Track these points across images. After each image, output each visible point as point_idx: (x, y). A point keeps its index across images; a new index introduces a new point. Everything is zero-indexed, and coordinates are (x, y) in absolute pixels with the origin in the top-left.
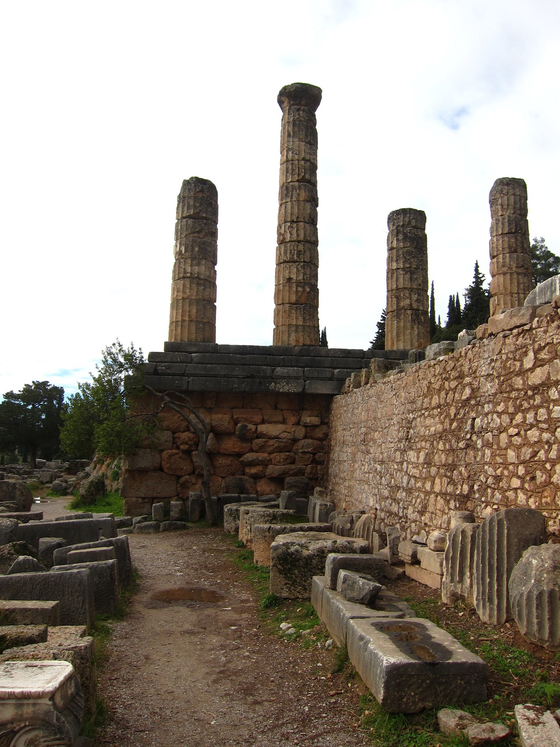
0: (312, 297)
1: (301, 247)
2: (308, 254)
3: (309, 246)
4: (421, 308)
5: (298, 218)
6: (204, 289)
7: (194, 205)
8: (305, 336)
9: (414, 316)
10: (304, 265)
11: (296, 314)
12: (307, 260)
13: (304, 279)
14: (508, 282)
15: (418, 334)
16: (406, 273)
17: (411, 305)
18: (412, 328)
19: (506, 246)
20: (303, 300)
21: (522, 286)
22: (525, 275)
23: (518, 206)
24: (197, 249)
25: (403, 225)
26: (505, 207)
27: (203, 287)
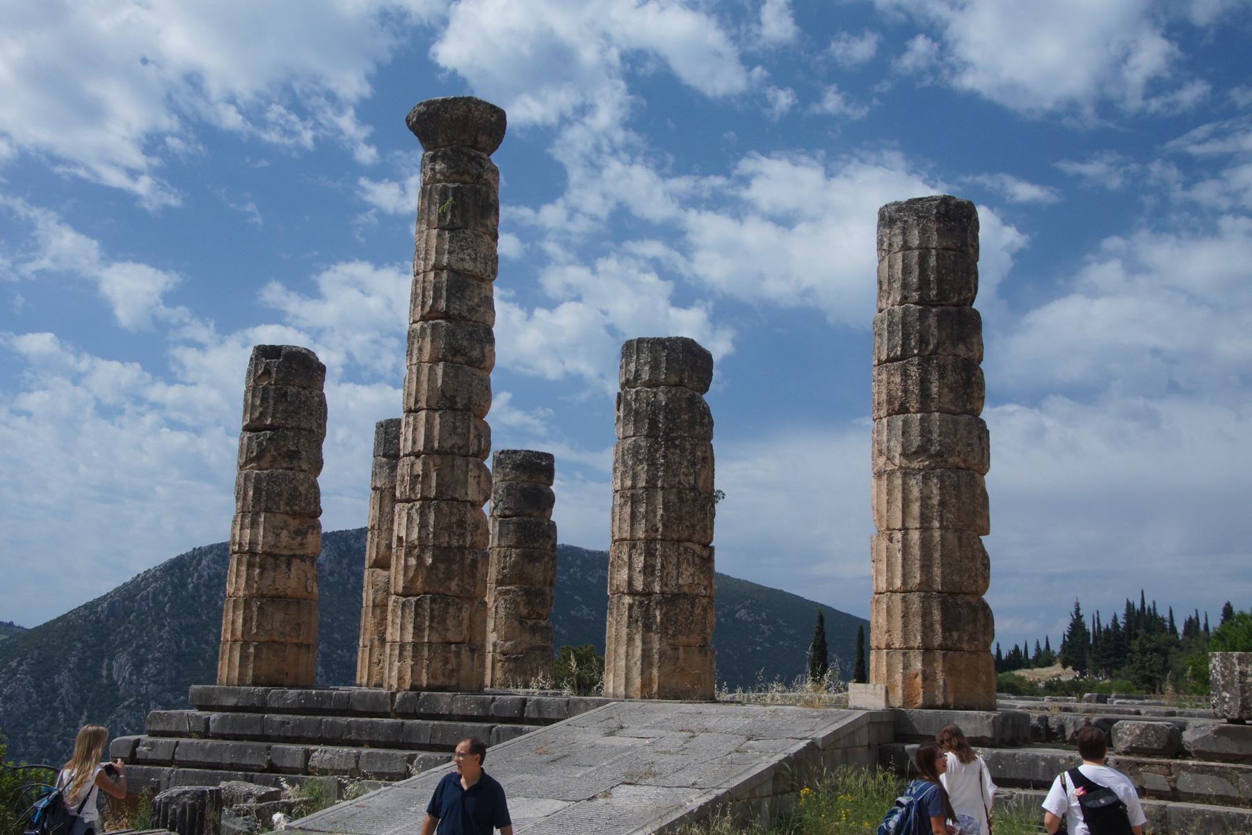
0: (441, 576)
3: (438, 460)
5: (417, 402)
6: (261, 574)
7: (253, 403)
9: (636, 611)
11: (403, 617)
13: (419, 538)
14: (885, 497)
16: (625, 503)
17: (630, 581)
18: (630, 639)
19: (884, 396)
21: (916, 508)
23: (914, 279)
24: (251, 493)
25: (627, 380)
26: (885, 287)
27: (257, 571)
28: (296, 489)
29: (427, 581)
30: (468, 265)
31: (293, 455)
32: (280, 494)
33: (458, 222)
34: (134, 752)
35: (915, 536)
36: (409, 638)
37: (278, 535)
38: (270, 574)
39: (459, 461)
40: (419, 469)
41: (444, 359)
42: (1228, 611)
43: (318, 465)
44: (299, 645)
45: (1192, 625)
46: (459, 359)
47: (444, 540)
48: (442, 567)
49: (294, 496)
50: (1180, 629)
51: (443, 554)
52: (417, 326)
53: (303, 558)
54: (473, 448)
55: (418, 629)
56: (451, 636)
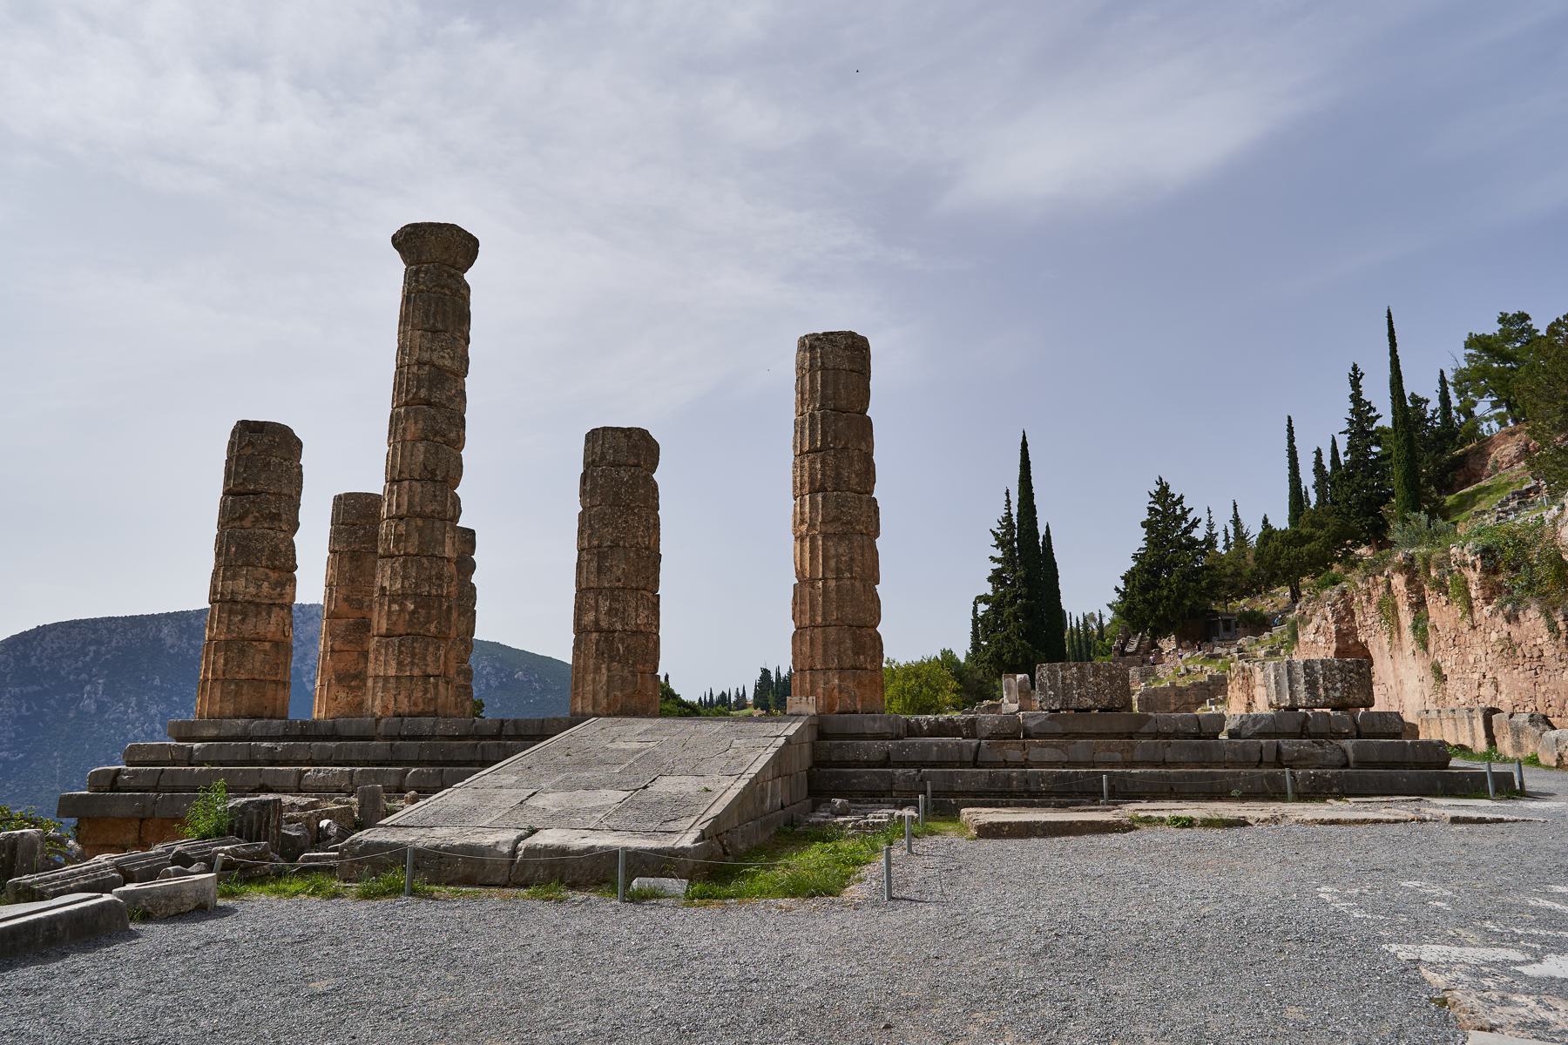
1: (402, 528)
2: (415, 539)
3: (420, 522)
4: (619, 627)
6: (243, 620)
8: (400, 698)
9: (602, 645)
10: (405, 561)
12: (410, 550)
14: (807, 555)
15: (610, 679)
17: (597, 622)
18: (597, 670)
20: (401, 629)
21: (832, 563)
22: (842, 536)
28: (277, 546)
29: (410, 623)
30: (448, 363)
31: (275, 517)
32: (262, 550)
33: (440, 326)
34: (114, 781)
35: (832, 583)
36: (392, 672)
37: (260, 586)
38: (251, 621)
39: (438, 524)
40: (402, 528)
41: (426, 438)
43: (295, 526)
44: (276, 682)
46: (438, 439)
47: (425, 589)
48: (422, 612)
49: (275, 552)
51: (424, 602)
53: (282, 607)
54: (450, 514)
55: (400, 664)
56: (430, 670)
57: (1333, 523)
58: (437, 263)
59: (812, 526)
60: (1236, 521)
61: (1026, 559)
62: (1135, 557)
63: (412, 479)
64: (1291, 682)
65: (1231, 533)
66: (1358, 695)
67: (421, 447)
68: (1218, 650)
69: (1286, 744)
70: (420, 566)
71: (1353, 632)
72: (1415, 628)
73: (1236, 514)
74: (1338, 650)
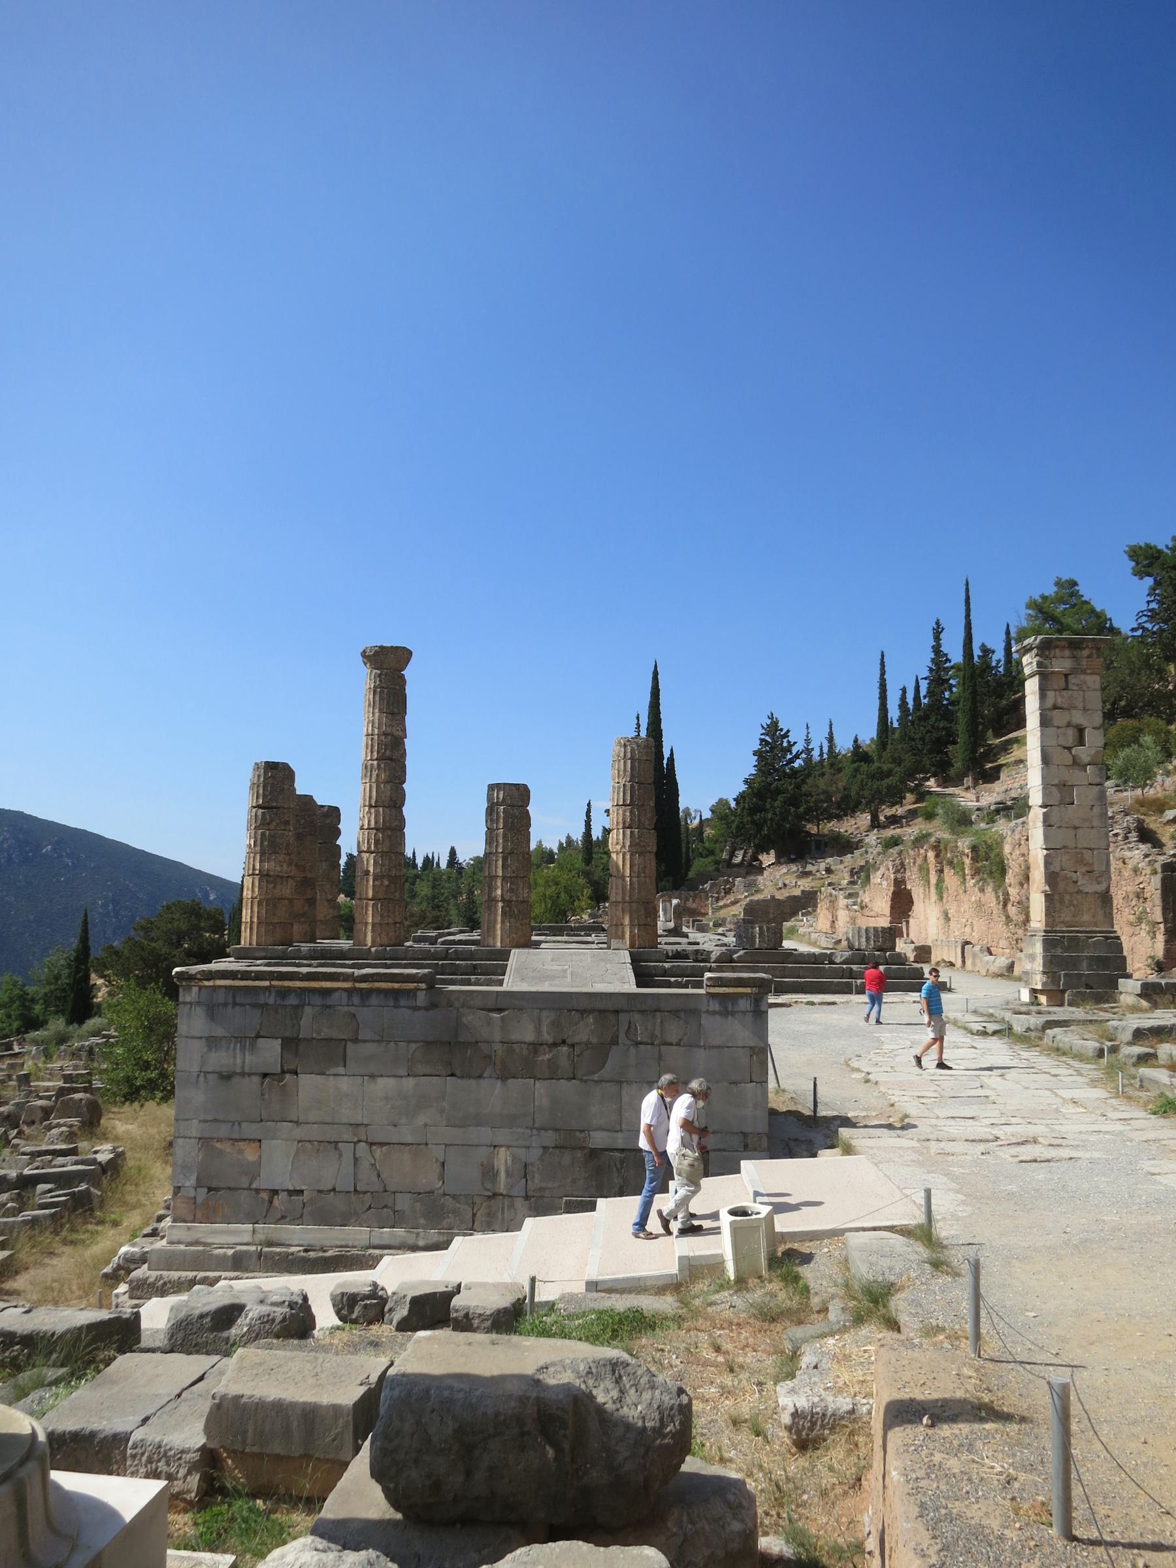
3: (389, 832)
19: (620, 819)
30: (400, 733)
33: (396, 710)
35: (635, 879)
42: (453, 853)
45: (428, 861)
47: (393, 872)
50: (420, 862)
52: (375, 763)
55: (382, 916)
57: (908, 759)
58: (389, 668)
59: (624, 846)
60: (831, 739)
61: (651, 776)
62: (746, 781)
63: (384, 807)
64: (860, 937)
65: (825, 750)
66: (888, 945)
67: (388, 786)
68: (809, 868)
69: (854, 967)
70: (390, 859)
71: (903, 882)
72: (937, 885)
73: (831, 734)
74: (894, 893)
